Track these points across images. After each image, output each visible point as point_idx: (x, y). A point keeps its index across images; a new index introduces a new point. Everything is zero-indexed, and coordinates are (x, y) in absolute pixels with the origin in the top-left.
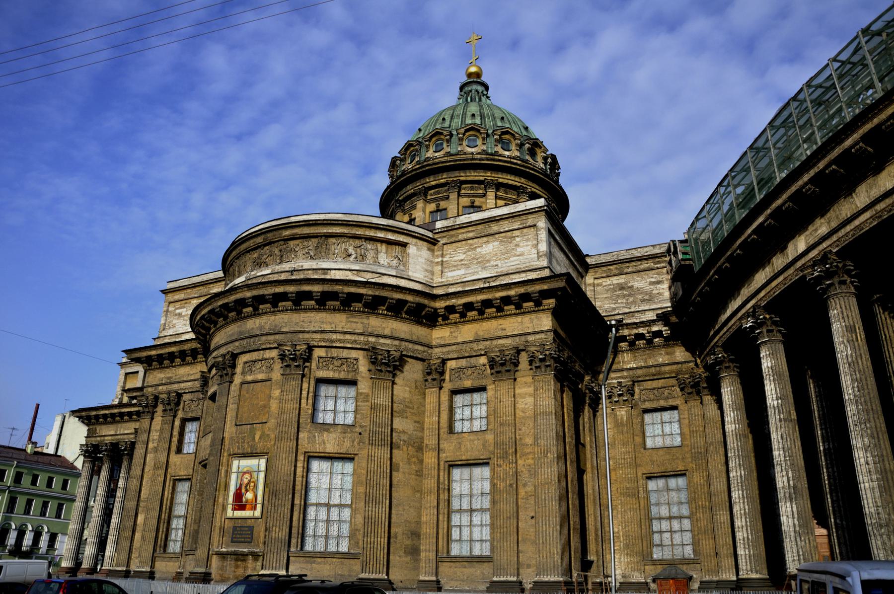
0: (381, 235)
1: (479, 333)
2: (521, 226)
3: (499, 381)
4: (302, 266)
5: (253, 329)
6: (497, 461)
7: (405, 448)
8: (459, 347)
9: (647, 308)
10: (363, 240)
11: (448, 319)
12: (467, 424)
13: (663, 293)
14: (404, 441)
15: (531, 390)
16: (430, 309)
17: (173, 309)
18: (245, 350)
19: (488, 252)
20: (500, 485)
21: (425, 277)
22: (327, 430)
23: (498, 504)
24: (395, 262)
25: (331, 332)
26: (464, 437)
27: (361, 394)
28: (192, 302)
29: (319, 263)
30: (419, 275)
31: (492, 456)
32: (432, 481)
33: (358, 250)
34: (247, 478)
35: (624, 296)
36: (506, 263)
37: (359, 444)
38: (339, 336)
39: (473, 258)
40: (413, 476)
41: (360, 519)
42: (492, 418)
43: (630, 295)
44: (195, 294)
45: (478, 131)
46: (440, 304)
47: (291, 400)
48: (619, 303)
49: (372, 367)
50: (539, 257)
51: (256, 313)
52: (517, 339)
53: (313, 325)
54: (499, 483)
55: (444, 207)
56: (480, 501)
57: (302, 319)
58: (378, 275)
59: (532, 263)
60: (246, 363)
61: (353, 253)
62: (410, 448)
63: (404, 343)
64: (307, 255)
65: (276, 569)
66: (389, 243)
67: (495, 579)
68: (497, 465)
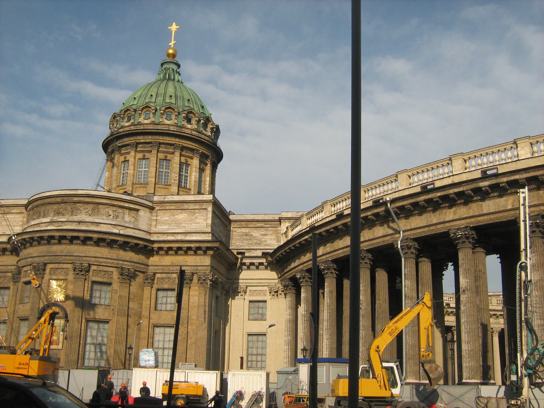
0: (127, 205)
2: (200, 208)
4: (85, 220)
5: (56, 251)
7: (133, 317)
9: (258, 248)
10: (117, 207)
11: (158, 253)
12: (164, 306)
13: (267, 241)
15: (197, 293)
16: (150, 248)
18: (52, 262)
19: (181, 218)
26: (162, 313)
29: (94, 219)
30: (144, 227)
33: (115, 212)
35: (247, 240)
37: (112, 315)
43: (250, 239)
45: (173, 109)
47: (79, 292)
48: (244, 243)
49: (120, 277)
50: (207, 226)
52: (193, 267)
55: (148, 158)
56: (168, 344)
59: (203, 229)
61: (112, 214)
62: (136, 317)
64: (87, 213)
66: (130, 209)
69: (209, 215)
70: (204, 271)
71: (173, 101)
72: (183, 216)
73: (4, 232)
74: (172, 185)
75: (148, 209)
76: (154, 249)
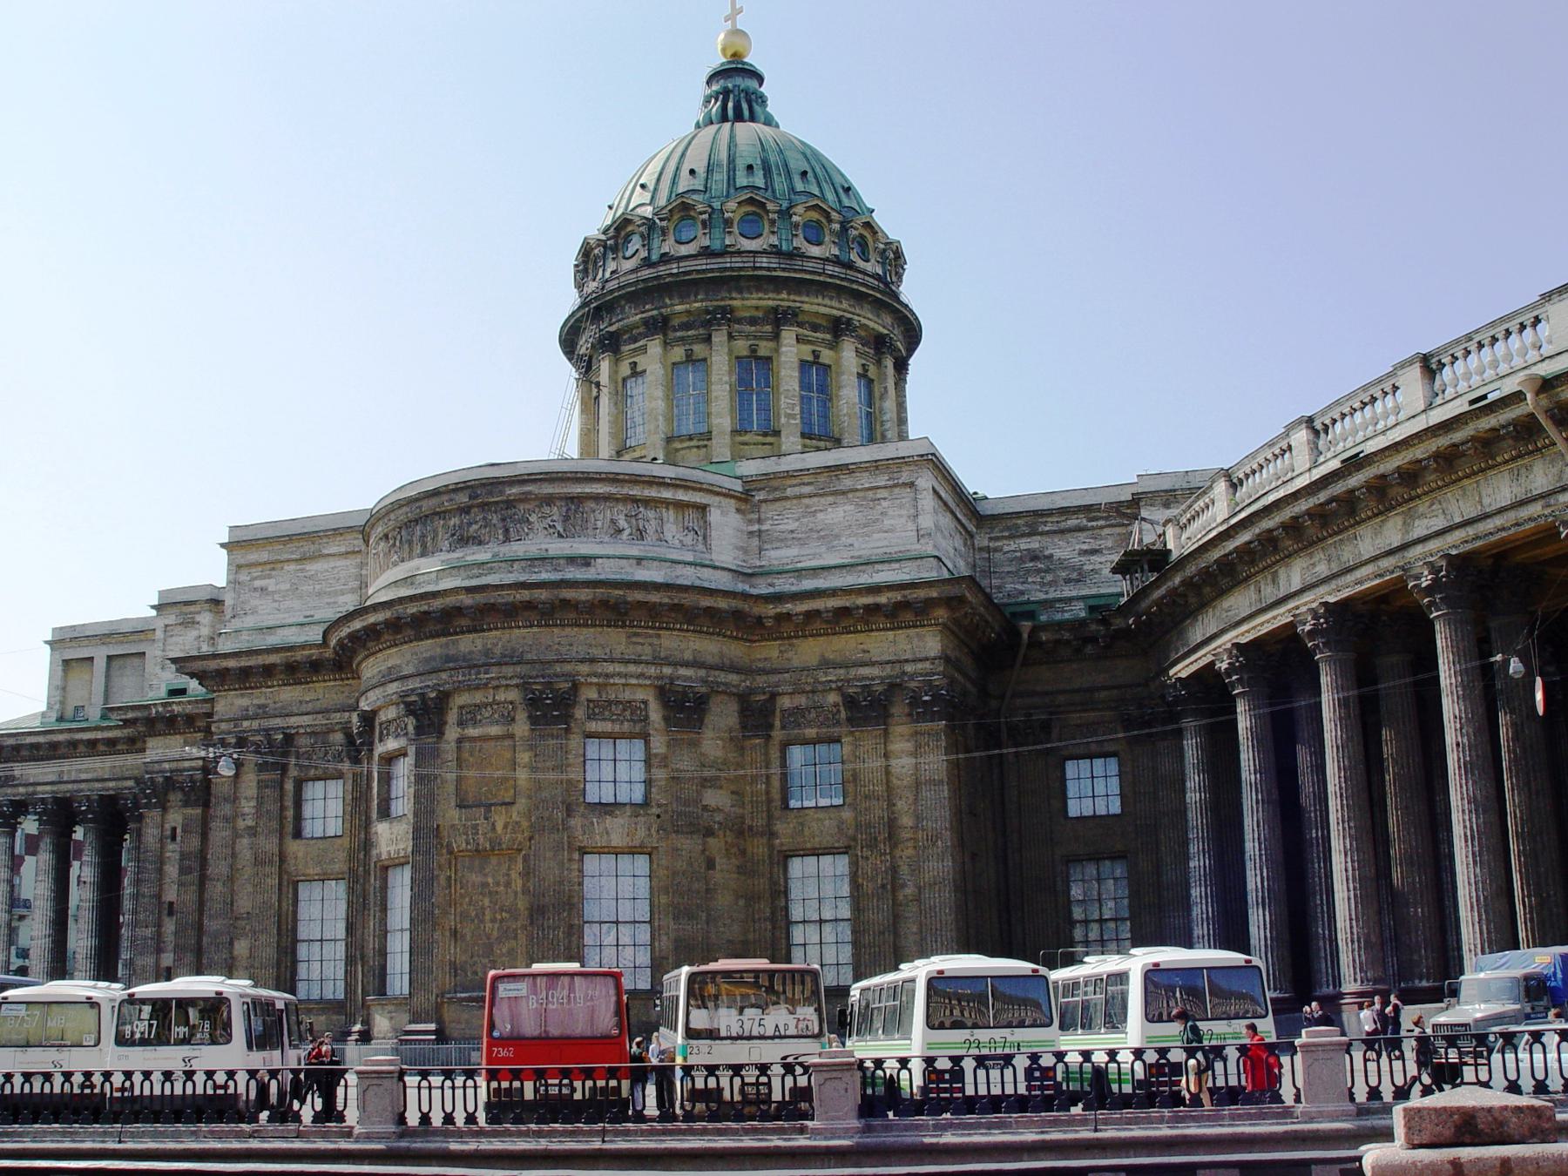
0: (667, 494)
1: (826, 655)
2: (891, 483)
5: (471, 652)
9: (1074, 593)
13: (1101, 569)
14: (720, 823)
17: (249, 578)
19: (836, 521)
22: (611, 814)
24: (689, 540)
31: (852, 843)
35: (1039, 571)
36: (867, 542)
38: (619, 668)
39: (811, 530)
40: (735, 876)
42: (850, 788)
43: (1048, 571)
44: (292, 553)
59: (908, 547)
60: (461, 707)
62: (728, 833)
63: (713, 672)
64: (552, 531)
68: (862, 857)
70: (926, 675)
71: (759, 181)
73: (308, 613)
74: (783, 434)
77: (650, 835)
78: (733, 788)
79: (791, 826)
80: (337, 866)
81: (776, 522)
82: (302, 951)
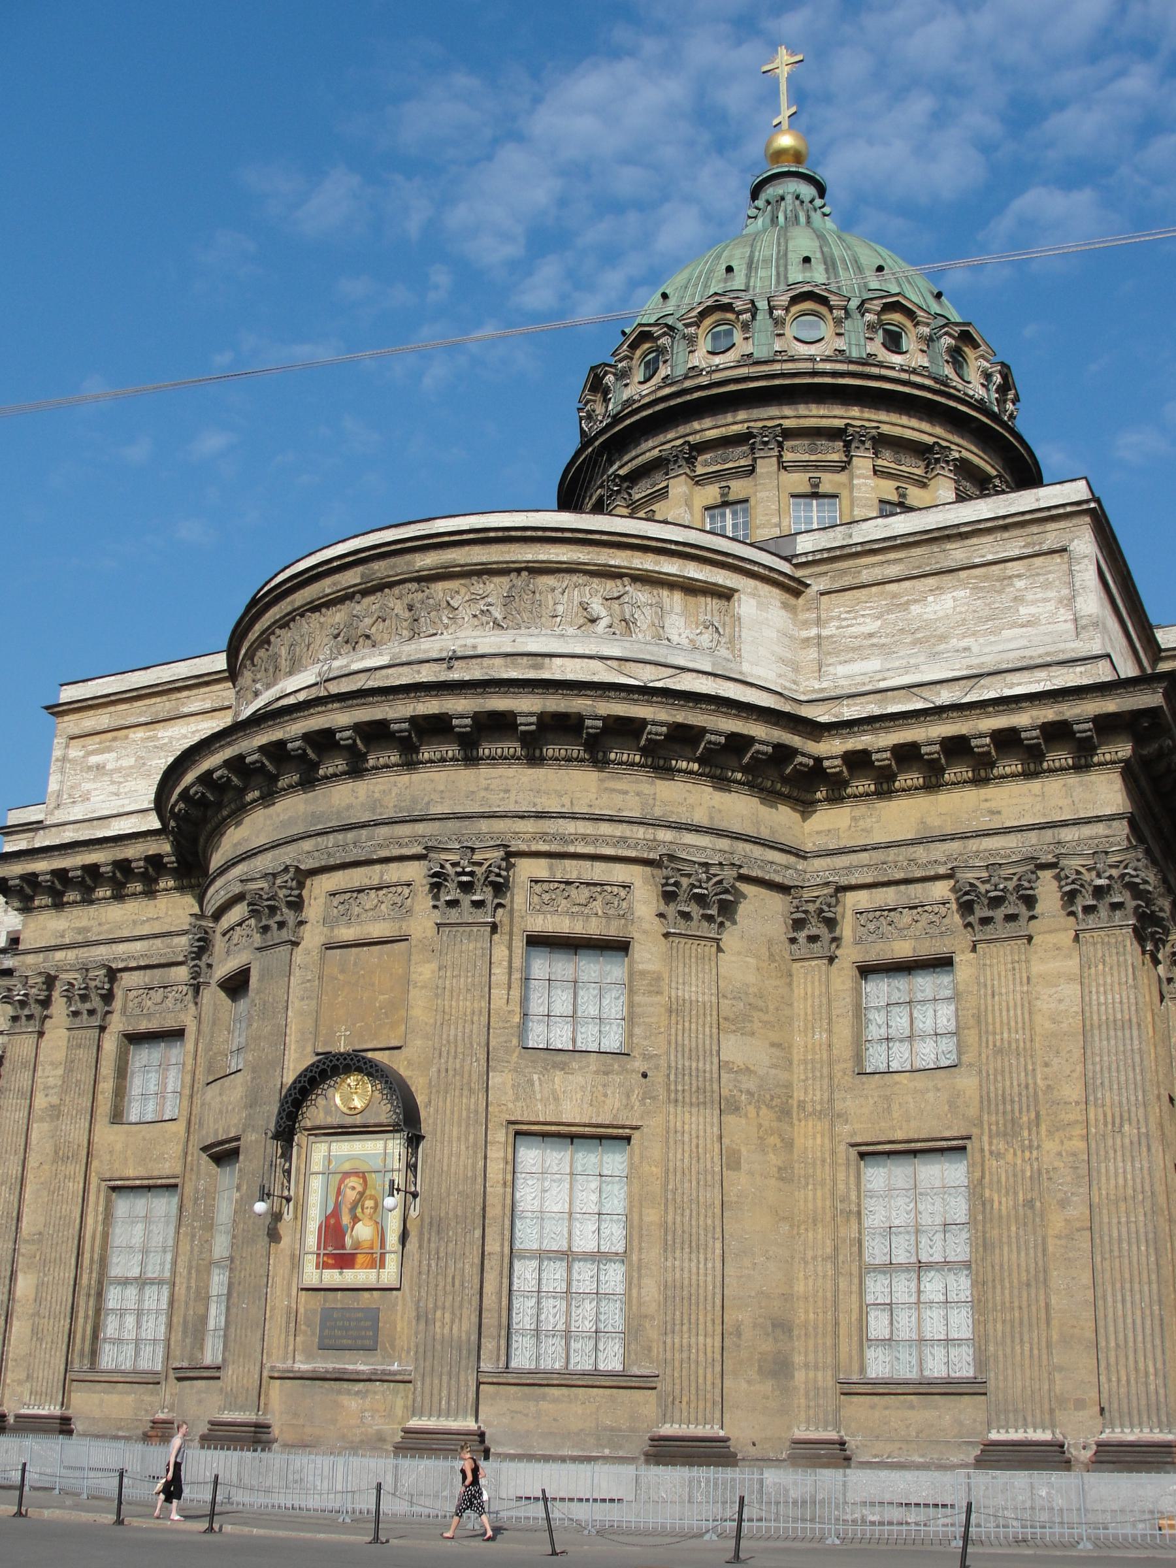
0: (670, 567)
1: (929, 820)
3: (989, 941)
4: (475, 647)
5: (349, 807)
6: (991, 1144)
7: (751, 1110)
8: (878, 856)
10: (626, 580)
15: (1072, 964)
16: (805, 760)
17: (81, 754)
18: (332, 862)
19: (941, 614)
20: (1000, 1203)
21: (780, 676)
22: (563, 1067)
23: (997, 1251)
24: (706, 639)
25: (562, 816)
26: (897, 1083)
27: (643, 973)
28: (132, 736)
29: (519, 640)
31: (975, 1131)
32: (819, 1193)
33: (615, 605)
34: (353, 1188)
37: (642, 1102)
40: (773, 1182)
41: (650, 1289)
42: (971, 1036)
44: (140, 715)
45: (824, 301)
46: (832, 748)
47: (468, 990)
51: (357, 770)
52: (1033, 837)
53: (513, 798)
54: (996, 1198)
55: (741, 497)
56: (939, 1244)
57: (484, 783)
58: (671, 671)
59: (1062, 646)
61: (603, 613)
62: (764, 1111)
64: (484, 619)
65: (448, 1415)
66: (691, 588)
67: (994, 1436)
68: (991, 1153)
69: (1078, 577)
72: (950, 603)
75: (776, 591)
76: (826, 763)
77: (629, 1106)
78: (774, 1036)
79: (871, 1101)
80: (167, 1165)
81: (844, 623)
82: (113, 1299)
